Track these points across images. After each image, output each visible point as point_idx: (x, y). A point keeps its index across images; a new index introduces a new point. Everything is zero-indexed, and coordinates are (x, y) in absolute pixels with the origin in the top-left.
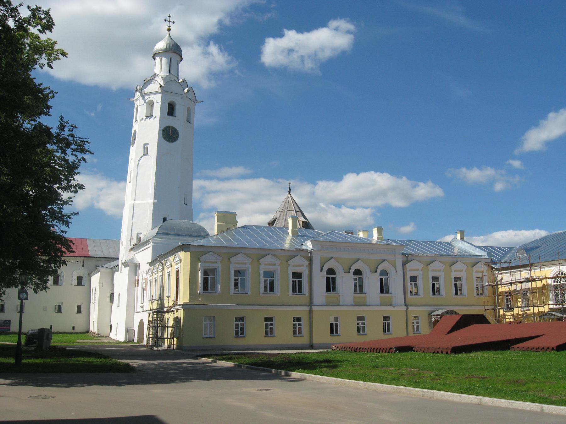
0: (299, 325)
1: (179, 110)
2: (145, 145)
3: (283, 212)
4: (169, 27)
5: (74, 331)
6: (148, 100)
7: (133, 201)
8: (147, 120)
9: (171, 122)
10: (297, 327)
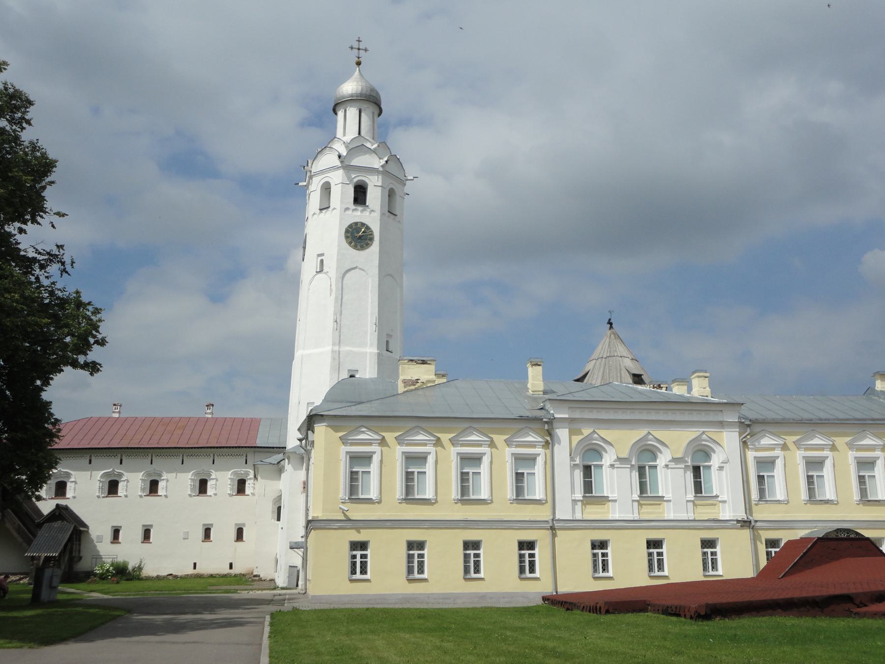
1: (374, 196)
2: (319, 255)
3: (600, 360)
6: (357, 180)
7: (341, 349)
8: (322, 215)
10: (710, 557)
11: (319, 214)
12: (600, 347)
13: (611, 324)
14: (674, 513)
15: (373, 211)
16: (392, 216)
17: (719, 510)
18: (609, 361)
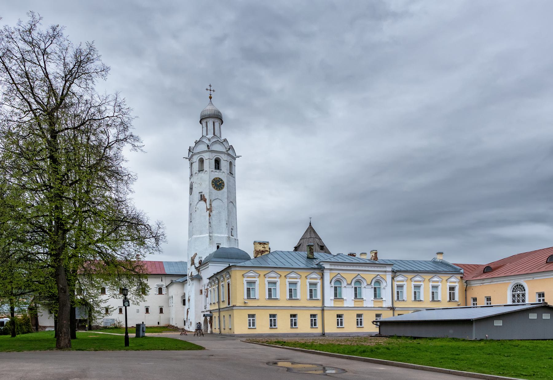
1: (224, 165)
2: (200, 193)
5: (159, 325)
15: (223, 172)
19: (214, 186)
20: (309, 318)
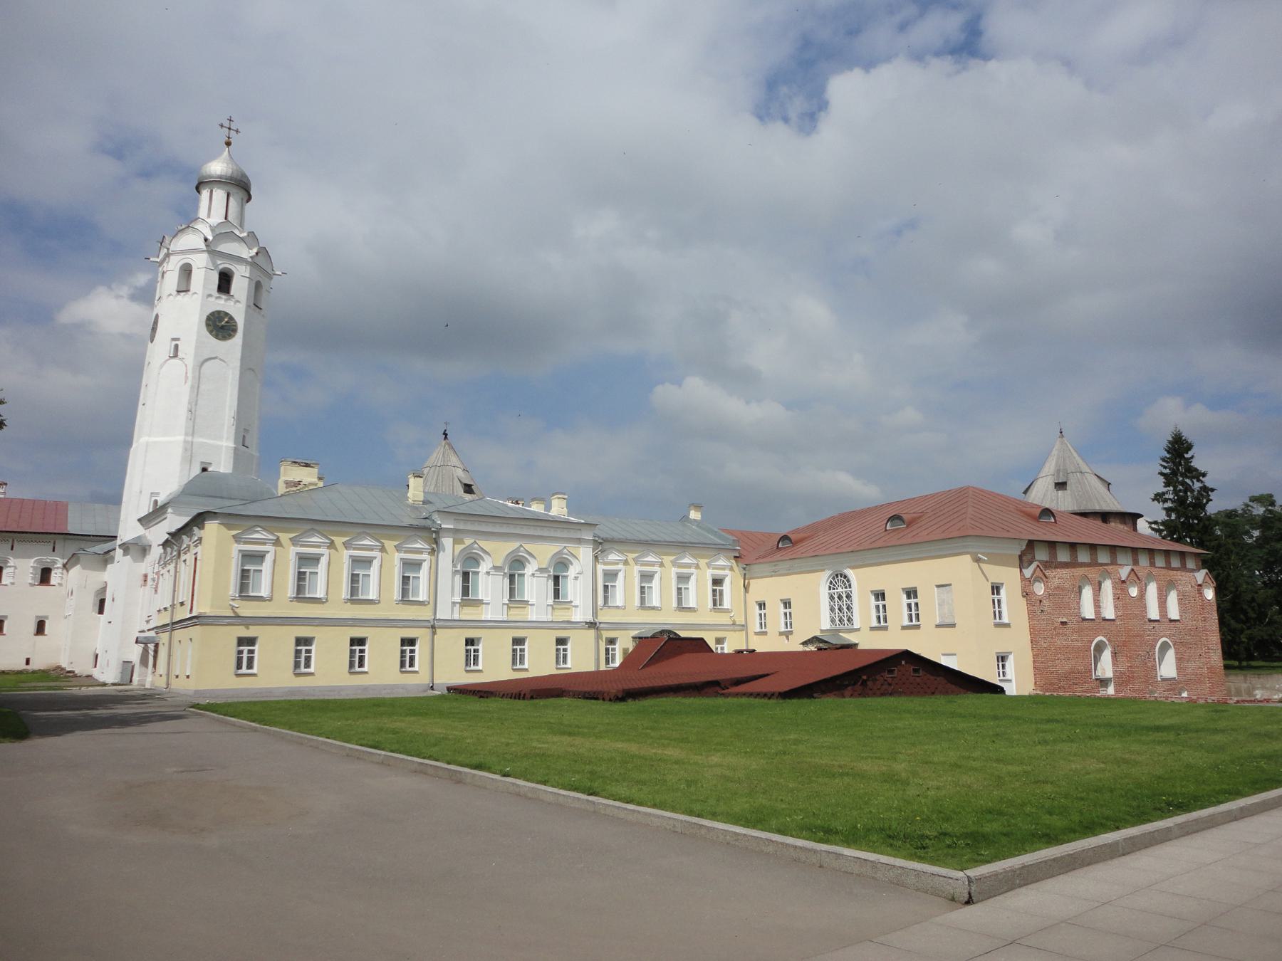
0: (521, 650)
1: (240, 285)
2: (173, 339)
4: (229, 138)
9: (221, 304)
11: (176, 296)
12: (435, 455)
13: (445, 434)
14: (491, 614)
15: (238, 301)
16: (258, 310)
17: (482, 610)
18: (442, 470)
19: (211, 328)
20: (509, 647)
